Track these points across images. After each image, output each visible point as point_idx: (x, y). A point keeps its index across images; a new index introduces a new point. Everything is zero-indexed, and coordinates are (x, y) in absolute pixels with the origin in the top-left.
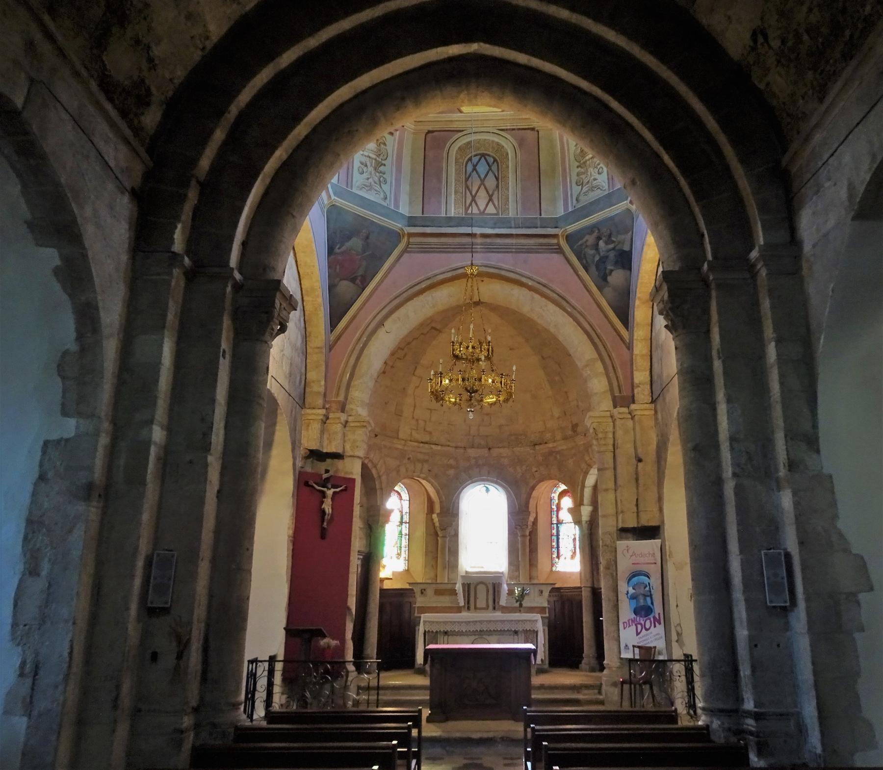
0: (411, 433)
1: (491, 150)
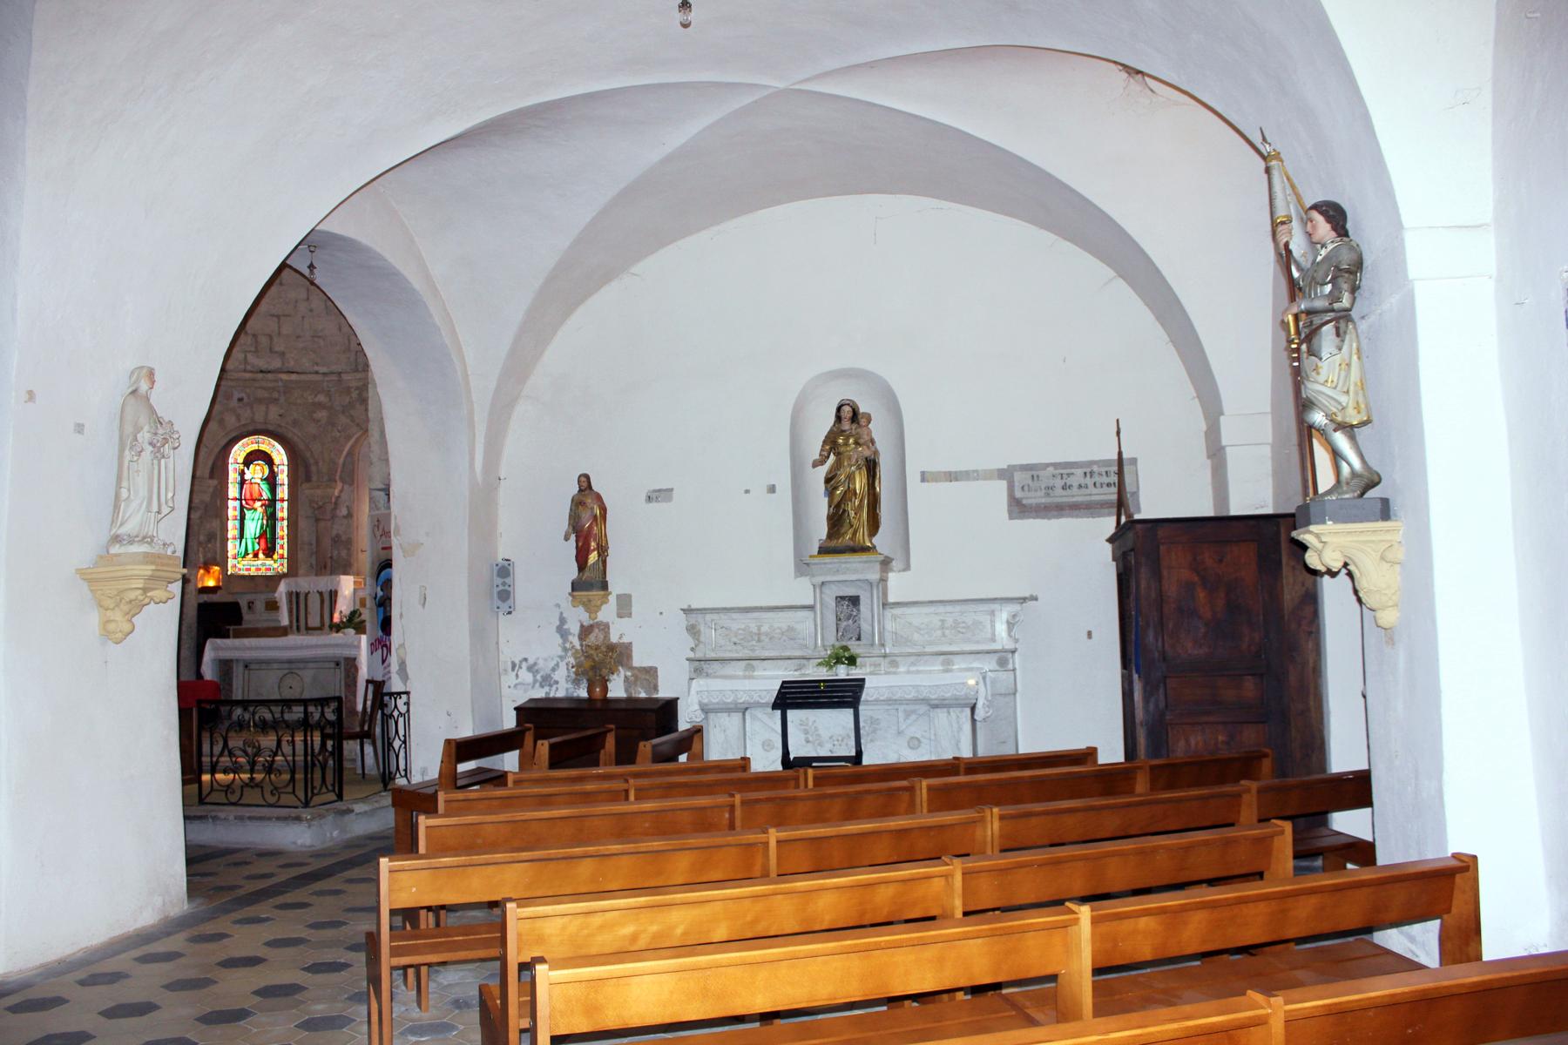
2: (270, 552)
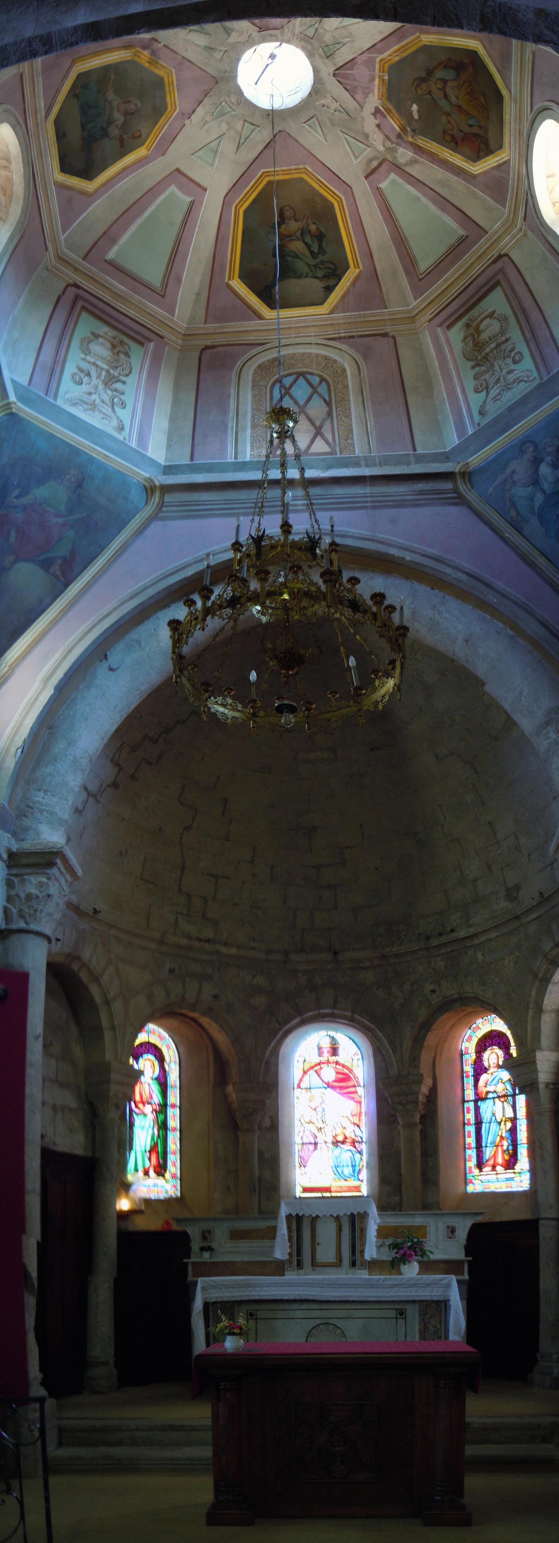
0: (176, 920)
1: (314, 366)
2: (161, 1170)
